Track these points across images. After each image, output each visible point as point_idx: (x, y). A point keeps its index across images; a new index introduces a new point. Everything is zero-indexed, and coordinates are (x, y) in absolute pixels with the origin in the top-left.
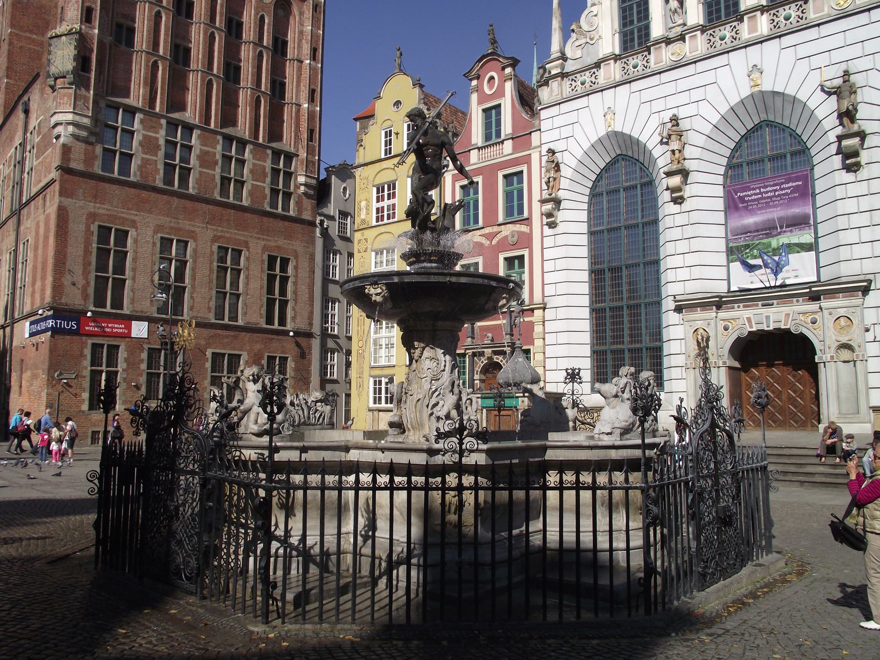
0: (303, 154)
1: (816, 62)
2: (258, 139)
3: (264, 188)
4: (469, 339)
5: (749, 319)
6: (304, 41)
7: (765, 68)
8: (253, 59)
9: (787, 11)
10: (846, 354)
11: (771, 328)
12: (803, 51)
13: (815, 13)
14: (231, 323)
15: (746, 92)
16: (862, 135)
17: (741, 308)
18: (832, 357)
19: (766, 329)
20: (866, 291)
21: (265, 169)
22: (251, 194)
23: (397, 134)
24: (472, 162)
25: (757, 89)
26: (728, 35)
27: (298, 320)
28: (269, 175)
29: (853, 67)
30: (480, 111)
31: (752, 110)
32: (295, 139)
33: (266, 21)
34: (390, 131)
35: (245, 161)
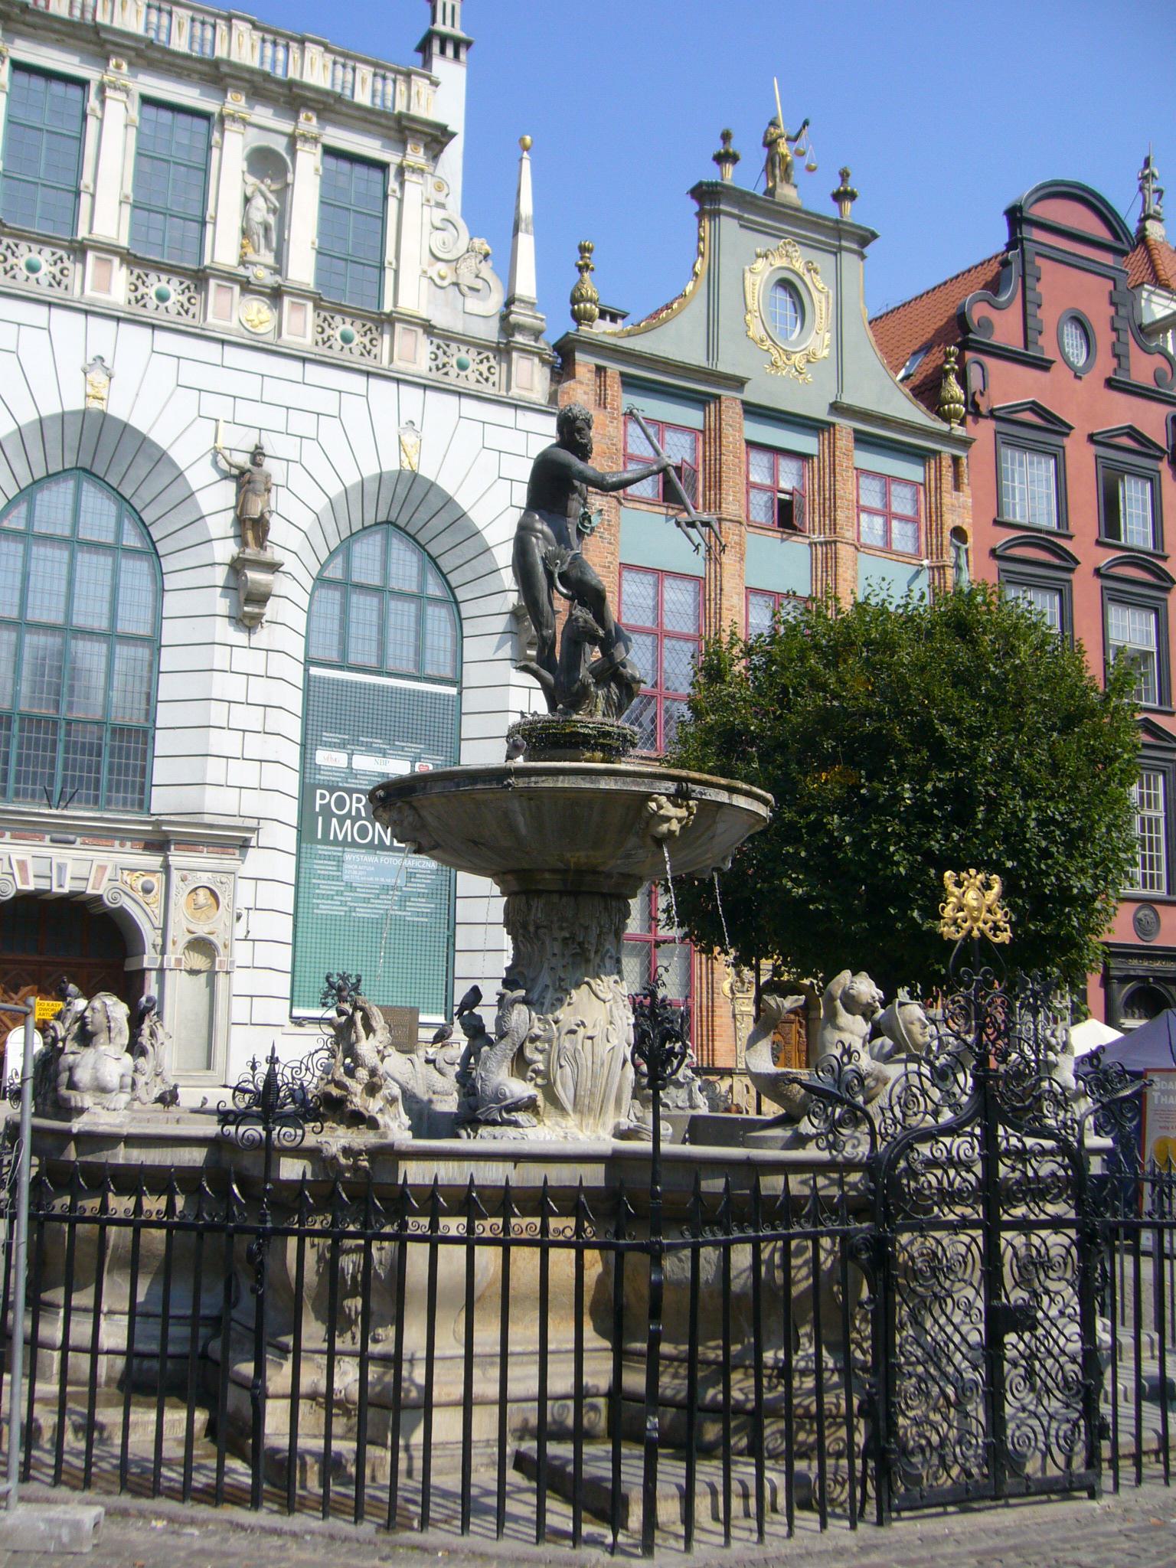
1: (213, 406)
5: (22, 865)
7: (117, 371)
9: (163, 284)
10: (199, 961)
11: (66, 890)
12: (192, 374)
13: (216, 316)
15: (75, 402)
16: (273, 567)
17: (47, 842)
18: (179, 961)
19: (56, 889)
20: (244, 845)
25: (95, 405)
26: (45, 268)
29: (273, 445)
31: (72, 439)
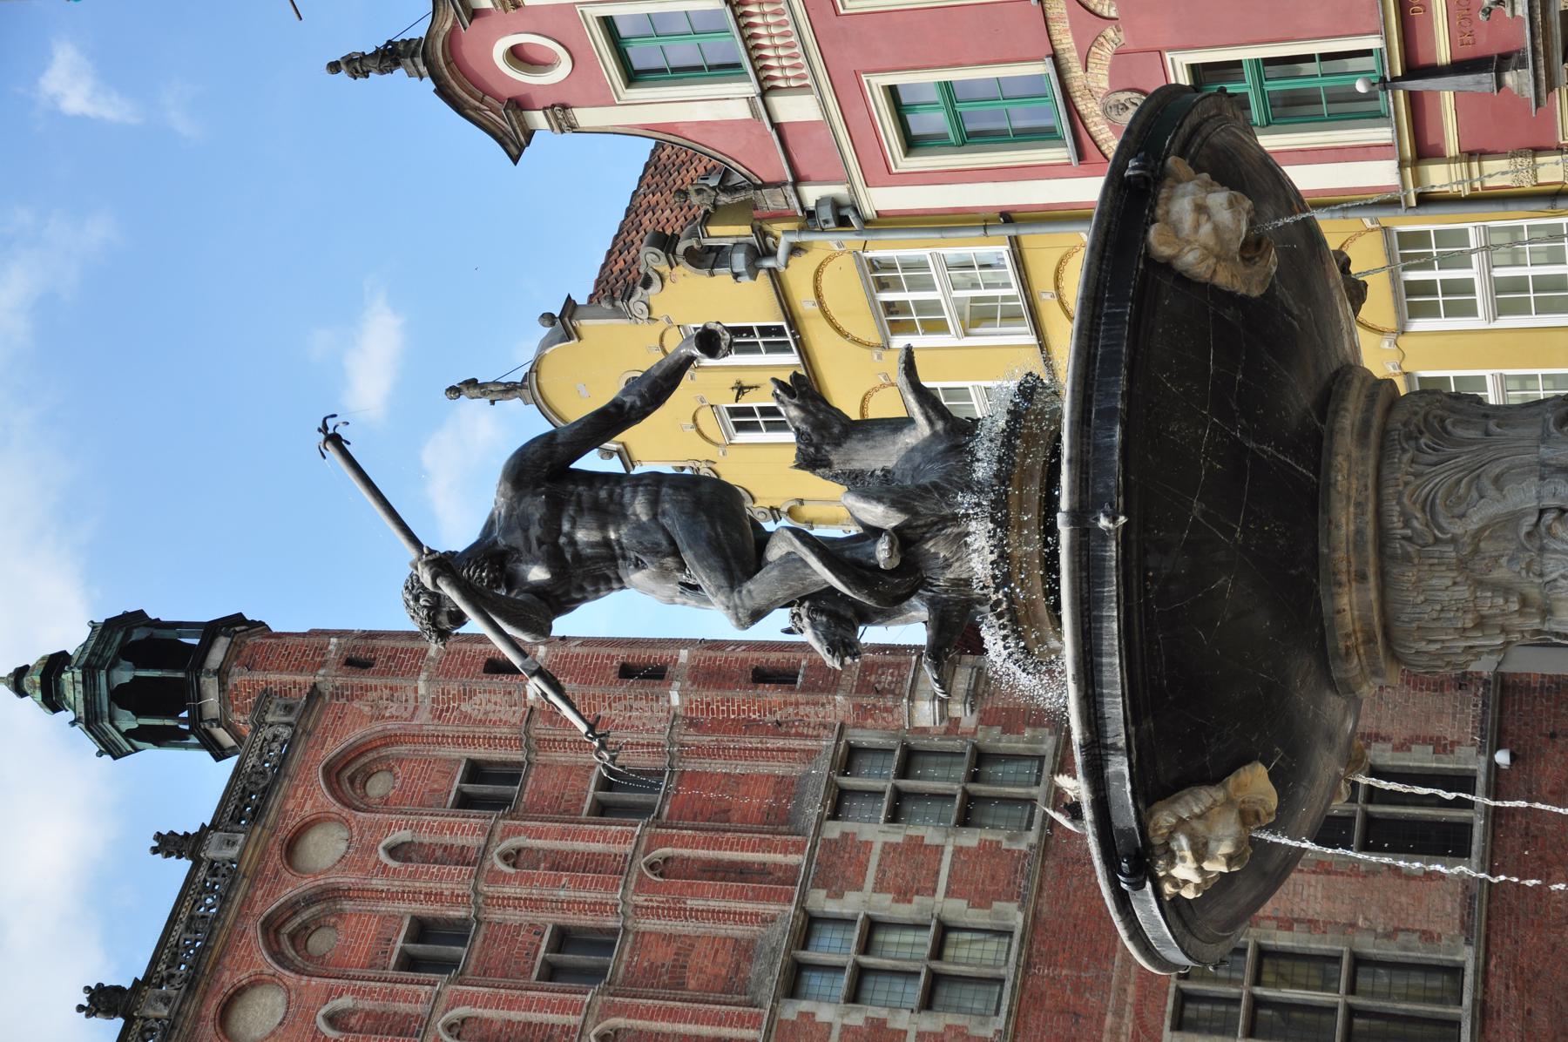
0: (840, 704)
2: (788, 876)
3: (958, 851)
4: (1509, 78)
6: (465, 707)
8: (527, 880)
14: (1467, 1000)
21: (895, 846)
22: (982, 900)
23: (741, 389)
24: (815, 115)
27: (1446, 729)
28: (913, 831)
30: (637, 93)
32: (787, 735)
33: (404, 835)
34: (734, 412)
35: (867, 917)
